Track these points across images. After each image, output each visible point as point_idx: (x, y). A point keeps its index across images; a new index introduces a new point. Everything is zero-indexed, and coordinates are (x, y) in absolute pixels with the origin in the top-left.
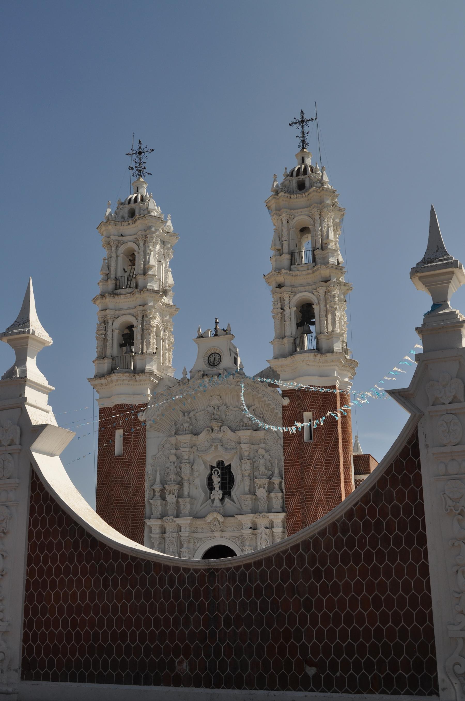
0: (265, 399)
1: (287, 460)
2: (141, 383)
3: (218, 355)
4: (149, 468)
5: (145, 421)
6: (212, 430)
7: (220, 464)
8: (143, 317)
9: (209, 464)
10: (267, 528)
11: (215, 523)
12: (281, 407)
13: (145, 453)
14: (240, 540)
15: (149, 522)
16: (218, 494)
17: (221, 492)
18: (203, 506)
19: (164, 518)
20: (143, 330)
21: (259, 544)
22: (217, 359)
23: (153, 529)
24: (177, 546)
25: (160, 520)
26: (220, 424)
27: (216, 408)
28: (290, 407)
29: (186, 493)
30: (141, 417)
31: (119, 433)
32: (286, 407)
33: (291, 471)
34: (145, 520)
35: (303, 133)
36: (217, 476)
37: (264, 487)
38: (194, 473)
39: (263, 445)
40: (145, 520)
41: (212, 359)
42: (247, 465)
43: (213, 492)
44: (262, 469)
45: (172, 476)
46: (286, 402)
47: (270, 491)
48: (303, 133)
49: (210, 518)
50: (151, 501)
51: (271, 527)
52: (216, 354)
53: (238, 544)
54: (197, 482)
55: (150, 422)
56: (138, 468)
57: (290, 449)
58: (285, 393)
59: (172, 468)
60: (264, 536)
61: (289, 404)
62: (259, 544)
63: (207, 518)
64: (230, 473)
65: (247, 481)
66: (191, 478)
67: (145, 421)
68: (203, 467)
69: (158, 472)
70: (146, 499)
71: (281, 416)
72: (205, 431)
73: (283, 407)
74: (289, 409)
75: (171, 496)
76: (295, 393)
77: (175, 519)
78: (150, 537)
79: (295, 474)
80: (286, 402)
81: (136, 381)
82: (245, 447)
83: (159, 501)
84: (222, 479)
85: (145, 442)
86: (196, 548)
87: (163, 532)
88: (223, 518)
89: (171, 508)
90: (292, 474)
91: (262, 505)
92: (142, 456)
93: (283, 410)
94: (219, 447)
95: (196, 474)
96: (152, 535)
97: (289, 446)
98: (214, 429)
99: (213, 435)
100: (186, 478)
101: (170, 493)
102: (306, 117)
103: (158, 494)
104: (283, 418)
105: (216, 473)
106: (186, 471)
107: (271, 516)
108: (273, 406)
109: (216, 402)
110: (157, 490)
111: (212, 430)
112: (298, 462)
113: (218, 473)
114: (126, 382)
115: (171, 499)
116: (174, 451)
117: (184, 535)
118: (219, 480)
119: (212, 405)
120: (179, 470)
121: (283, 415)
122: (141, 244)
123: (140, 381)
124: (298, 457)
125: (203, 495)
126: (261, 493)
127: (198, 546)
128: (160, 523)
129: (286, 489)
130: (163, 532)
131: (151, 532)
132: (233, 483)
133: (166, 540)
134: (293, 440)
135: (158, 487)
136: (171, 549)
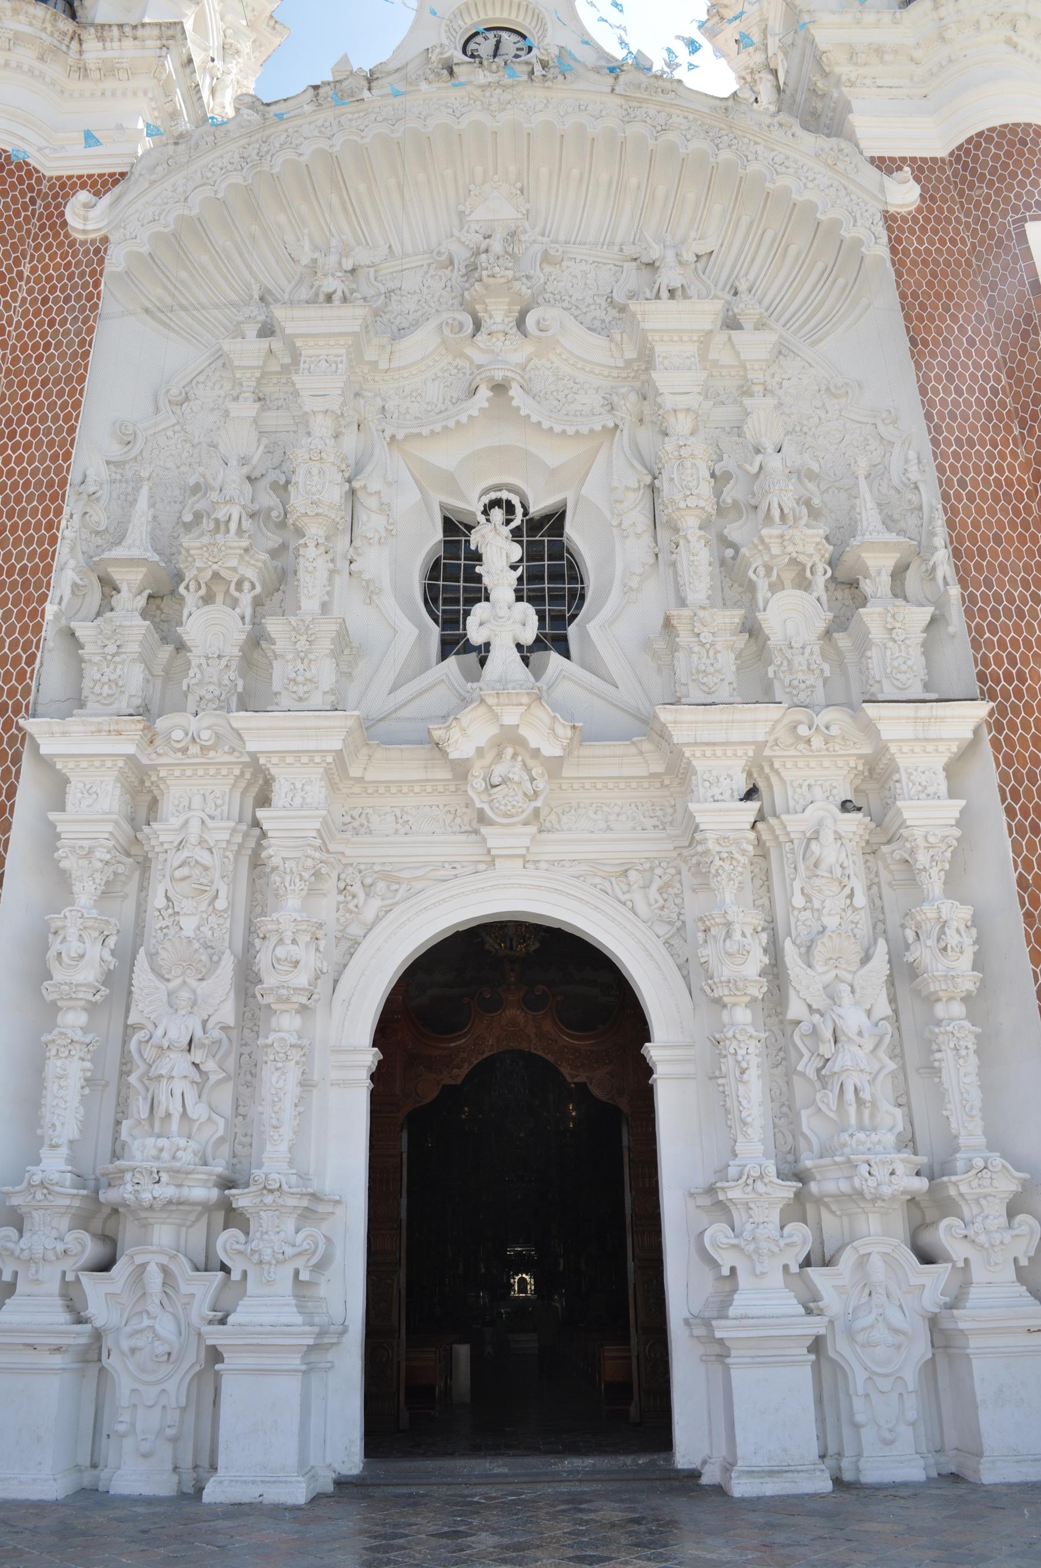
0: (782, 181)
1: (948, 443)
2: (109, 84)
3: (515, 38)
4: (91, 457)
5: (105, 240)
6: (478, 326)
9: (438, 498)
10: (845, 806)
11: (499, 771)
12: (878, 216)
13: (81, 379)
14: (657, 883)
15: (48, 735)
16: (503, 619)
17: (527, 611)
19: (161, 724)
21: (798, 901)
23: (71, 789)
24: (232, 904)
25: (135, 726)
28: (927, 220)
29: (310, 605)
32: (904, 219)
33: (983, 496)
36: (506, 531)
37: (804, 584)
38: (362, 516)
43: (479, 610)
46: (905, 194)
50: (84, 630)
51: (871, 796)
52: (505, 35)
53: (642, 908)
54: (375, 562)
56: (27, 447)
57: (959, 392)
59: (233, 478)
60: (829, 853)
61: (919, 210)
62: (798, 901)
63: (455, 733)
64: (560, 551)
65: (698, 558)
66: (342, 543)
67: (105, 240)
68: (420, 496)
69: (144, 492)
70: (50, 609)
71: (885, 252)
72: (432, 325)
73: (889, 218)
74: (923, 230)
75: (218, 610)
76: (942, 170)
77: (240, 719)
78: (51, 838)
79: (1004, 511)
81: (83, 71)
82: (677, 383)
83: (137, 628)
84: (532, 553)
85: (91, 331)
86: (355, 930)
87: (143, 801)
90: (992, 512)
92: (60, 394)
93: (889, 229)
95: (371, 522)
96: (65, 824)
97: (950, 378)
98: (487, 324)
100: (315, 530)
101: (208, 599)
103: (129, 601)
104: (898, 264)
105: (498, 514)
106: (316, 491)
107: (894, 723)
109: (497, 208)
110: (130, 580)
111: (478, 326)
112: (1014, 455)
114: (26, 56)
115: (211, 630)
117: (288, 824)
118: (516, 552)
119: (474, 226)
120: (268, 499)
121: (893, 251)
123: (109, 70)
124: (1009, 430)
125: (408, 632)
126: (793, 616)
127: (369, 915)
128: (130, 749)
129: (963, 582)
130: (143, 801)
131: (60, 806)
132: (578, 598)
133: (156, 866)
134: (968, 354)
136: (189, 925)
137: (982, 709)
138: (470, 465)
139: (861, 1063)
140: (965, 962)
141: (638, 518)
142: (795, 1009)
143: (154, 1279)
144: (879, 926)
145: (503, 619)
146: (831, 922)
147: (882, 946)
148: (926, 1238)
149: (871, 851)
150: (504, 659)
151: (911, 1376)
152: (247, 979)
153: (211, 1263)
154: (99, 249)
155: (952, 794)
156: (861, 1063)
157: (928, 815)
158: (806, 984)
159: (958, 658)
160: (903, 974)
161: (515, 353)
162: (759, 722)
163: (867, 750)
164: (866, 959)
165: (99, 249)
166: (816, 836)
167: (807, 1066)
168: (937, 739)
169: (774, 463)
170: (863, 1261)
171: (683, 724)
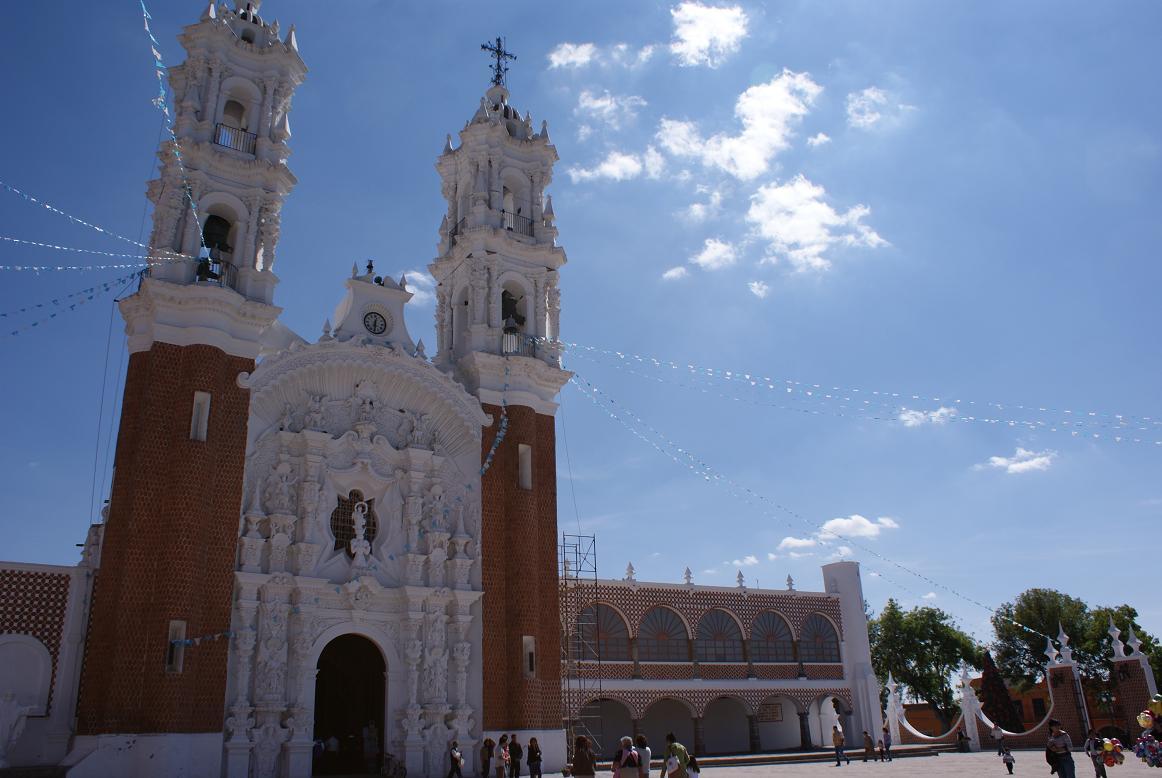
7: (356, 495)
8: (260, 211)
18: (333, 560)
20: (260, 233)
22: (380, 323)
26: (375, 429)
27: (368, 402)
29: (308, 535)
30: (243, 381)
31: (202, 399)
34: (236, 573)
35: (499, 67)
37: (441, 546)
39: (439, 480)
40: (236, 573)
41: (371, 322)
42: (415, 504)
44: (439, 518)
45: (286, 501)
46: (488, 421)
47: (452, 554)
48: (499, 67)
49: (353, 586)
51: (451, 611)
55: (257, 394)
58: (487, 408)
65: (415, 532)
80: (488, 421)
82: (418, 478)
88: (380, 588)
89: (279, 556)
91: (438, 574)
94: (369, 467)
99: (357, 446)
102: (507, 47)
105: (360, 509)
108: (469, 424)
113: (363, 511)
115: (280, 540)
116: (284, 457)
118: (364, 522)
122: (270, 92)
126: (438, 555)
127: (319, 632)
135: (256, 515)
136: (274, 633)
137: (482, 593)
138: (346, 482)
139: (440, 681)
140: (466, 657)
141: (398, 514)
142: (426, 666)
143: (271, 731)
144: (447, 647)
145: (359, 545)
146: (436, 643)
147: (448, 651)
148: (450, 723)
149: (448, 623)
150: (359, 560)
151: (442, 756)
152: (291, 652)
153: (283, 727)
154: (246, 394)
155: (470, 614)
156: (440, 681)
157: (464, 620)
158: (429, 660)
159: (478, 579)
160: (452, 658)
161: (369, 447)
162: (427, 592)
163: (452, 599)
164: (444, 655)
165: (246, 394)
166: (436, 621)
167: (427, 681)
168: (469, 598)
169: (439, 506)
170: (436, 729)
171: (410, 591)
